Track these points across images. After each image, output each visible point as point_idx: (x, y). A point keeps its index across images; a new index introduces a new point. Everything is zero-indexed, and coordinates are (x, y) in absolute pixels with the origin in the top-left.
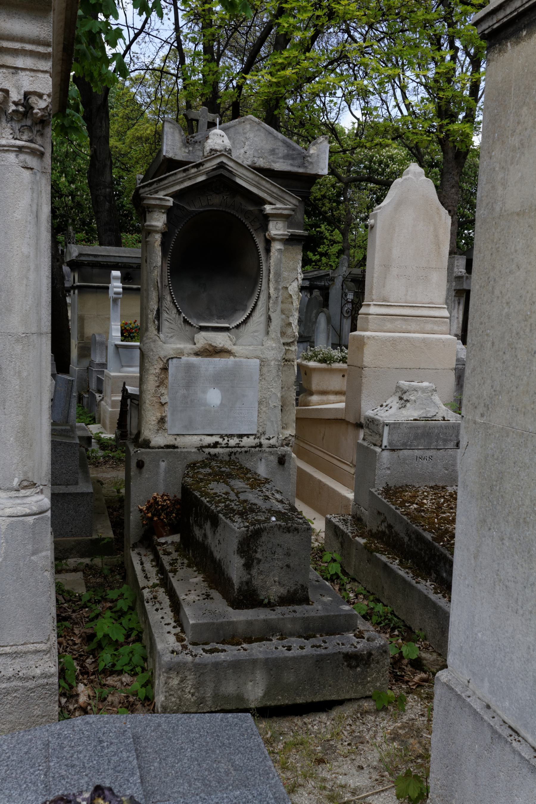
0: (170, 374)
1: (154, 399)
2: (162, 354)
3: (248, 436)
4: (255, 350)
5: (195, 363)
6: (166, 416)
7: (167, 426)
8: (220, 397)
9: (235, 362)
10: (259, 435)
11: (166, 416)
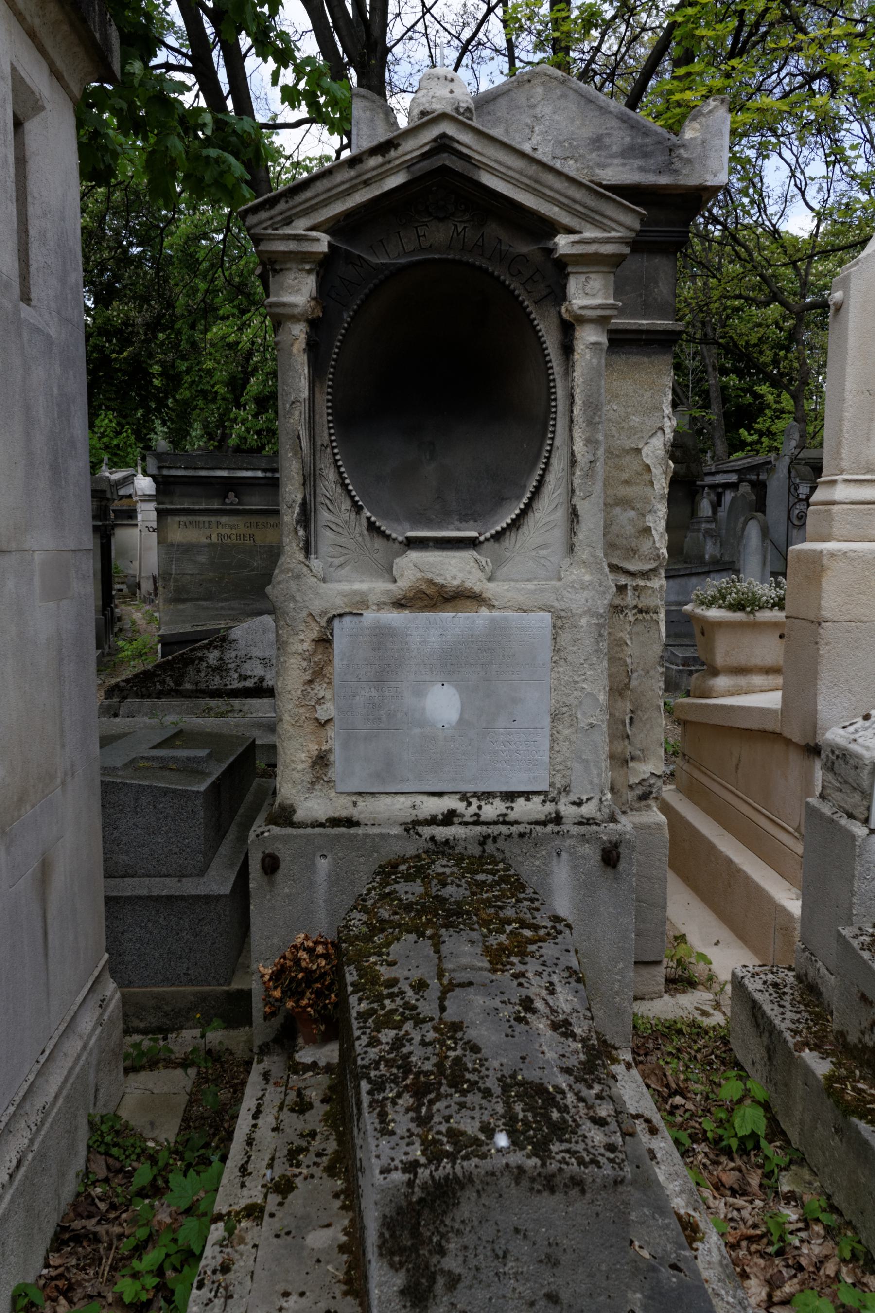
0: (336, 652)
1: (302, 710)
2: (316, 606)
3: (527, 795)
4: (542, 591)
5: (394, 624)
6: (330, 751)
7: (332, 773)
8: (458, 704)
9: (493, 620)
10: (554, 793)
11: (330, 751)
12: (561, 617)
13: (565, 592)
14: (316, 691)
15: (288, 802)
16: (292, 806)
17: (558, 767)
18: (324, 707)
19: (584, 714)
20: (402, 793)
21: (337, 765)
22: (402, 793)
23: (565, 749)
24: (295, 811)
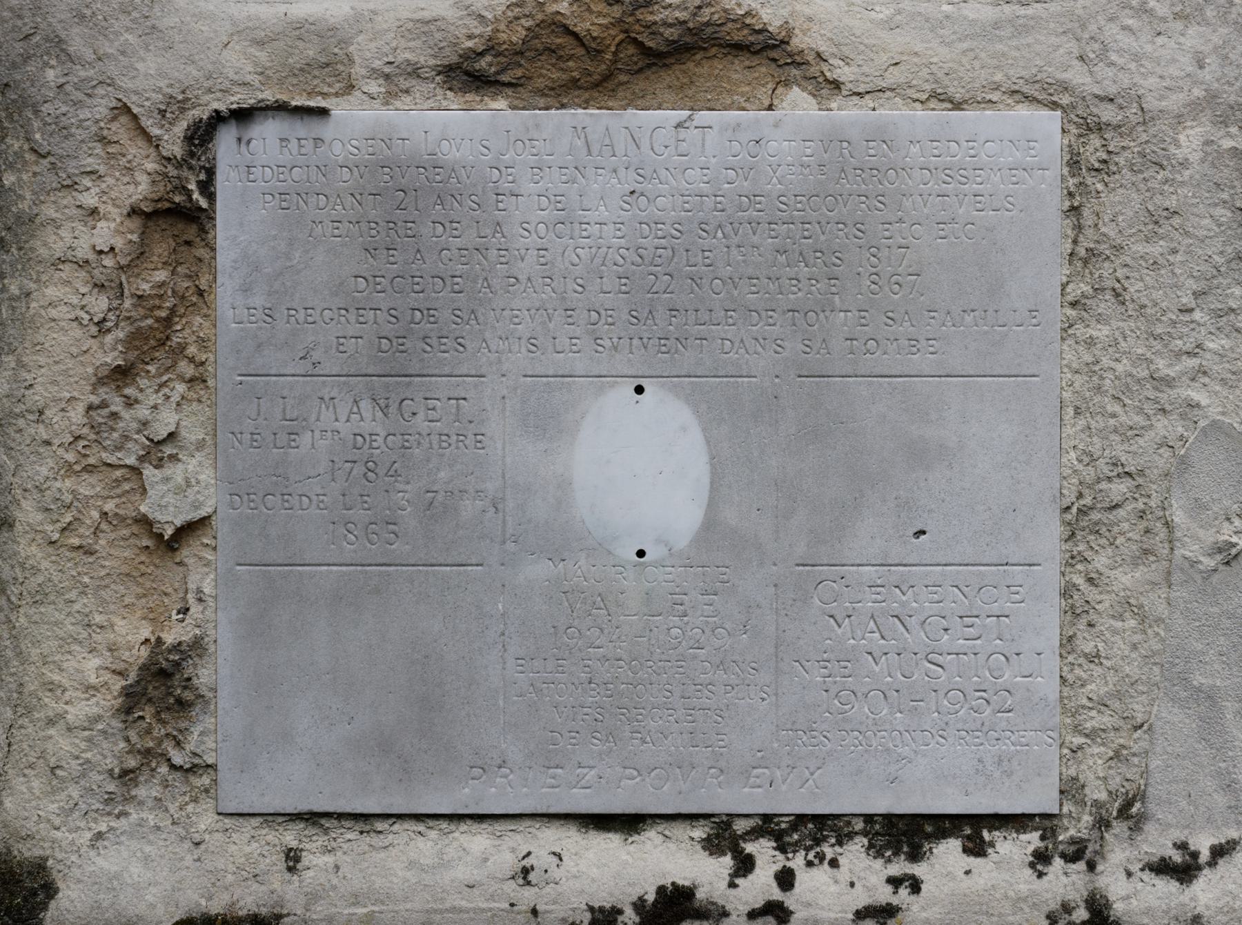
0: (225, 256)
1: (89, 486)
2: (148, 75)
3: (974, 831)
4: (1022, 28)
5: (450, 153)
6: (197, 646)
7: (206, 736)
8: (699, 468)
9: (834, 139)
10: (1077, 827)
11: (197, 646)
12: (1100, 128)
13: (1112, 30)
14: (143, 412)
15: (26, 851)
16: (40, 867)
17: (1095, 720)
18: (177, 472)
19: (1198, 507)
20: (480, 818)
21: (224, 701)
22: (480, 818)
23: (1120, 646)
24: (50, 890)
